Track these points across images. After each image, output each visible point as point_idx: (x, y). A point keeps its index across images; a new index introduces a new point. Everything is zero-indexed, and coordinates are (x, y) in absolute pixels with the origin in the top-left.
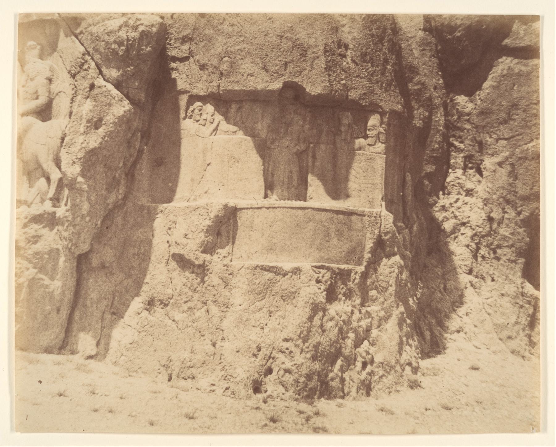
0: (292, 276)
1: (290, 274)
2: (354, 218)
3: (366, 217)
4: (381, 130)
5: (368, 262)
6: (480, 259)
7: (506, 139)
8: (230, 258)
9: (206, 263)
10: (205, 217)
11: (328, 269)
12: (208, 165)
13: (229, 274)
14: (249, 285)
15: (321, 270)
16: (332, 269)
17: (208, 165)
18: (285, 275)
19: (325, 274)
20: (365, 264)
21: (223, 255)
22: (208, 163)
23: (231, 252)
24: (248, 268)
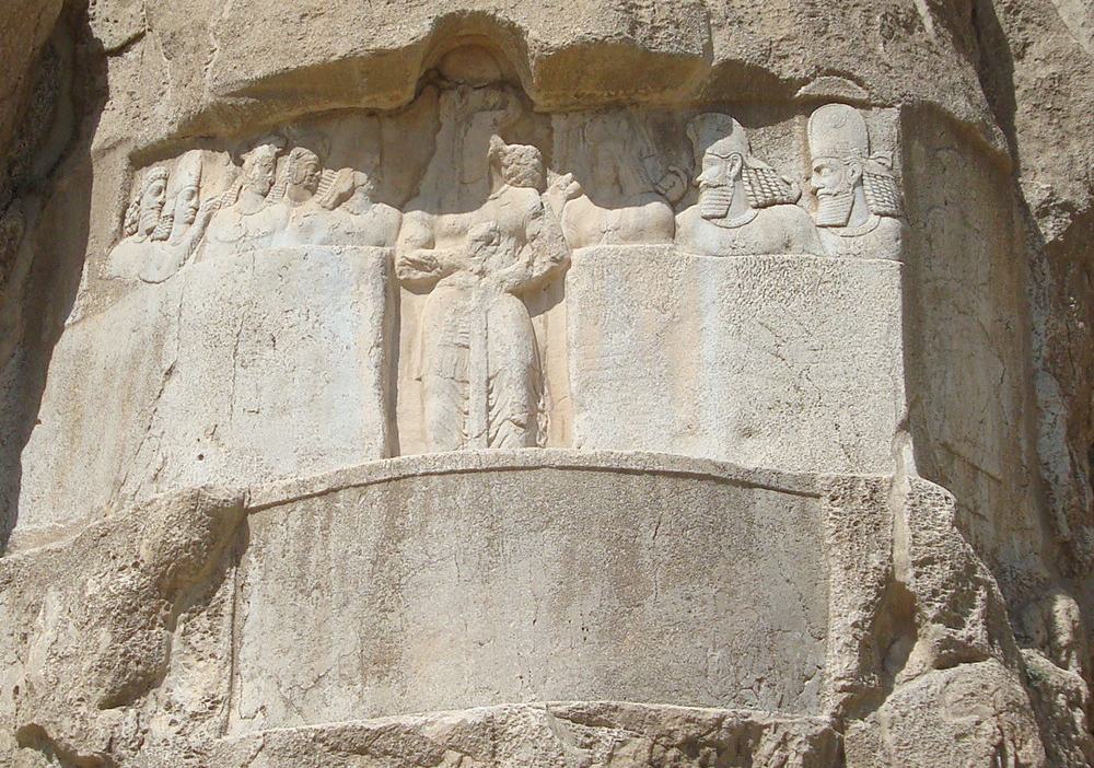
1: (453, 756)
2: (763, 502)
3: (825, 501)
4: (872, 165)
5: (844, 689)
8: (217, 718)
9: (120, 750)
10: (119, 562)
11: (635, 723)
12: (169, 373)
15: (602, 732)
17: (169, 373)
19: (623, 743)
20: (833, 701)
21: (189, 709)
22: (167, 367)
23: (222, 692)
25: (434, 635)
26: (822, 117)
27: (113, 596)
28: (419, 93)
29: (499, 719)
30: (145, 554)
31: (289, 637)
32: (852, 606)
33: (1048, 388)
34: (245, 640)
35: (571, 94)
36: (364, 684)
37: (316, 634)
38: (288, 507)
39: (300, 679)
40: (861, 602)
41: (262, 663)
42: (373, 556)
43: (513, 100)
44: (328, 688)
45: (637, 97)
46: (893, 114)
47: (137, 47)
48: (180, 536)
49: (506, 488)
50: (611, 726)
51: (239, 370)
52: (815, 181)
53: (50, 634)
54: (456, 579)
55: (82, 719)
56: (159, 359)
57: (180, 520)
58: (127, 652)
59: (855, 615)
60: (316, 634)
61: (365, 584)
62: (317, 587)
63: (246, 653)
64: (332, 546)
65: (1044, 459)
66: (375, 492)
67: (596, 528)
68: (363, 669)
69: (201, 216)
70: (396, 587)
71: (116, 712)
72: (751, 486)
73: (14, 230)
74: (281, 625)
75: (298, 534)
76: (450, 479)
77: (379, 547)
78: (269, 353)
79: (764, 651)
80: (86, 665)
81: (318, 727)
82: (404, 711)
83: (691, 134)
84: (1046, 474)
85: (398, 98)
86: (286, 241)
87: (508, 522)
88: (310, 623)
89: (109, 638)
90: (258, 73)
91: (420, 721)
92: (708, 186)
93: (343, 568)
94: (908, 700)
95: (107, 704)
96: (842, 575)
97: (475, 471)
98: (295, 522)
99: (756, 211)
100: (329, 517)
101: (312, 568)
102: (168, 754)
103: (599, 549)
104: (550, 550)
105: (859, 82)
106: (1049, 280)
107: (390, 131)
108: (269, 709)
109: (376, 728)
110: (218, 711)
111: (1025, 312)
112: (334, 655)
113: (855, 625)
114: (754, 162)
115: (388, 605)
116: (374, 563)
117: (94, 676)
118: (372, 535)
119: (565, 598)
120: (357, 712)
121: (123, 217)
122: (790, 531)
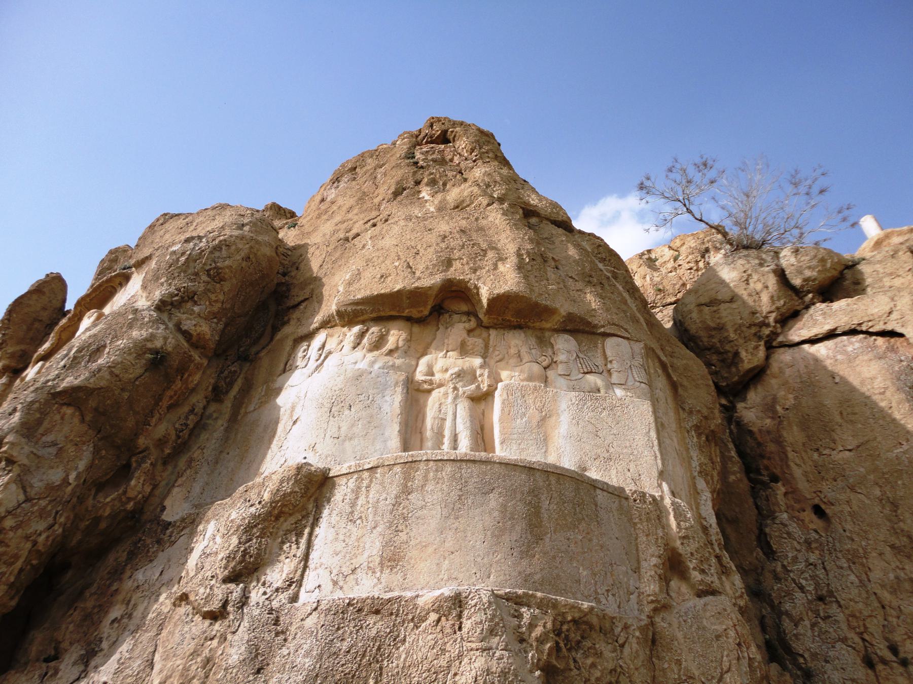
0: (439, 620)
1: (433, 617)
6: (880, 667)
7: (850, 450)
11: (543, 605)
12: (295, 423)
13: (277, 634)
14: (320, 656)
16: (555, 605)
18: (417, 621)
21: (275, 586)
22: (295, 418)
24: (329, 610)
25: (425, 546)
26: (610, 342)
27: (244, 518)
28: (431, 314)
29: (464, 595)
30: (266, 496)
31: (340, 546)
32: (653, 556)
33: (701, 484)
34: (315, 548)
35: (500, 318)
36: (382, 572)
37: (356, 544)
38: (349, 476)
39: (344, 569)
40: (657, 554)
41: (323, 560)
42: (393, 501)
43: (473, 319)
44: (360, 574)
45: (530, 324)
46: (642, 345)
47: (304, 304)
48: (287, 487)
49: (469, 471)
50: (529, 606)
51: (331, 418)
52: (609, 366)
53: (205, 543)
54: (439, 516)
55: (211, 589)
56: (291, 416)
57: (289, 479)
58: (246, 550)
59: (654, 561)
60: (356, 544)
61: (388, 517)
62: (361, 518)
63: (314, 555)
64: (371, 496)
65: (704, 515)
66: (398, 469)
67: (519, 496)
68: (381, 564)
69: (322, 357)
70: (405, 519)
71: (232, 586)
72: (595, 487)
73: (235, 371)
74: (336, 539)
75: (353, 491)
76: (440, 464)
77: (396, 497)
78: (347, 412)
79: (609, 574)
80: (220, 557)
81: (352, 596)
82: (405, 589)
83: (552, 341)
84: (705, 523)
85: (422, 311)
86: (363, 365)
87: (470, 487)
88: (354, 538)
89: (237, 542)
90: (359, 296)
91: (414, 594)
92: (561, 362)
93: (376, 508)
94: (685, 613)
95: (226, 580)
96: (645, 539)
97: (453, 460)
98: (352, 483)
99: (582, 375)
100: (371, 481)
101: (358, 508)
102: (258, 611)
103: (520, 507)
104: (493, 504)
105: (626, 330)
106: (695, 440)
107: (416, 329)
108: (322, 587)
109: (387, 597)
110: (292, 587)
111: (687, 450)
112: (366, 555)
113: (655, 565)
114: (581, 355)
115: (400, 528)
116: (394, 505)
117: (224, 562)
118: (394, 490)
119: (502, 531)
120: (376, 588)
121: (286, 364)
122: (615, 513)
